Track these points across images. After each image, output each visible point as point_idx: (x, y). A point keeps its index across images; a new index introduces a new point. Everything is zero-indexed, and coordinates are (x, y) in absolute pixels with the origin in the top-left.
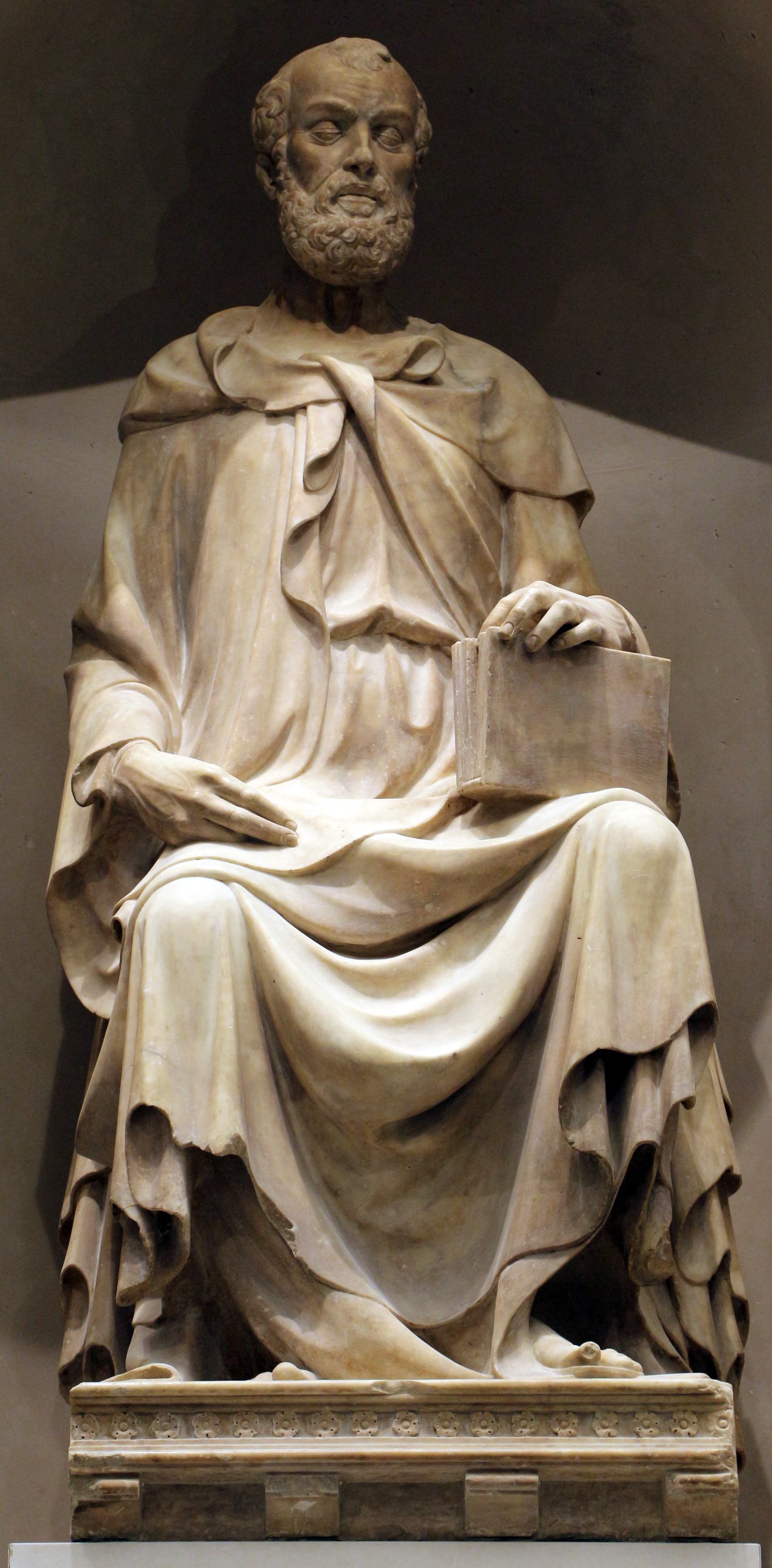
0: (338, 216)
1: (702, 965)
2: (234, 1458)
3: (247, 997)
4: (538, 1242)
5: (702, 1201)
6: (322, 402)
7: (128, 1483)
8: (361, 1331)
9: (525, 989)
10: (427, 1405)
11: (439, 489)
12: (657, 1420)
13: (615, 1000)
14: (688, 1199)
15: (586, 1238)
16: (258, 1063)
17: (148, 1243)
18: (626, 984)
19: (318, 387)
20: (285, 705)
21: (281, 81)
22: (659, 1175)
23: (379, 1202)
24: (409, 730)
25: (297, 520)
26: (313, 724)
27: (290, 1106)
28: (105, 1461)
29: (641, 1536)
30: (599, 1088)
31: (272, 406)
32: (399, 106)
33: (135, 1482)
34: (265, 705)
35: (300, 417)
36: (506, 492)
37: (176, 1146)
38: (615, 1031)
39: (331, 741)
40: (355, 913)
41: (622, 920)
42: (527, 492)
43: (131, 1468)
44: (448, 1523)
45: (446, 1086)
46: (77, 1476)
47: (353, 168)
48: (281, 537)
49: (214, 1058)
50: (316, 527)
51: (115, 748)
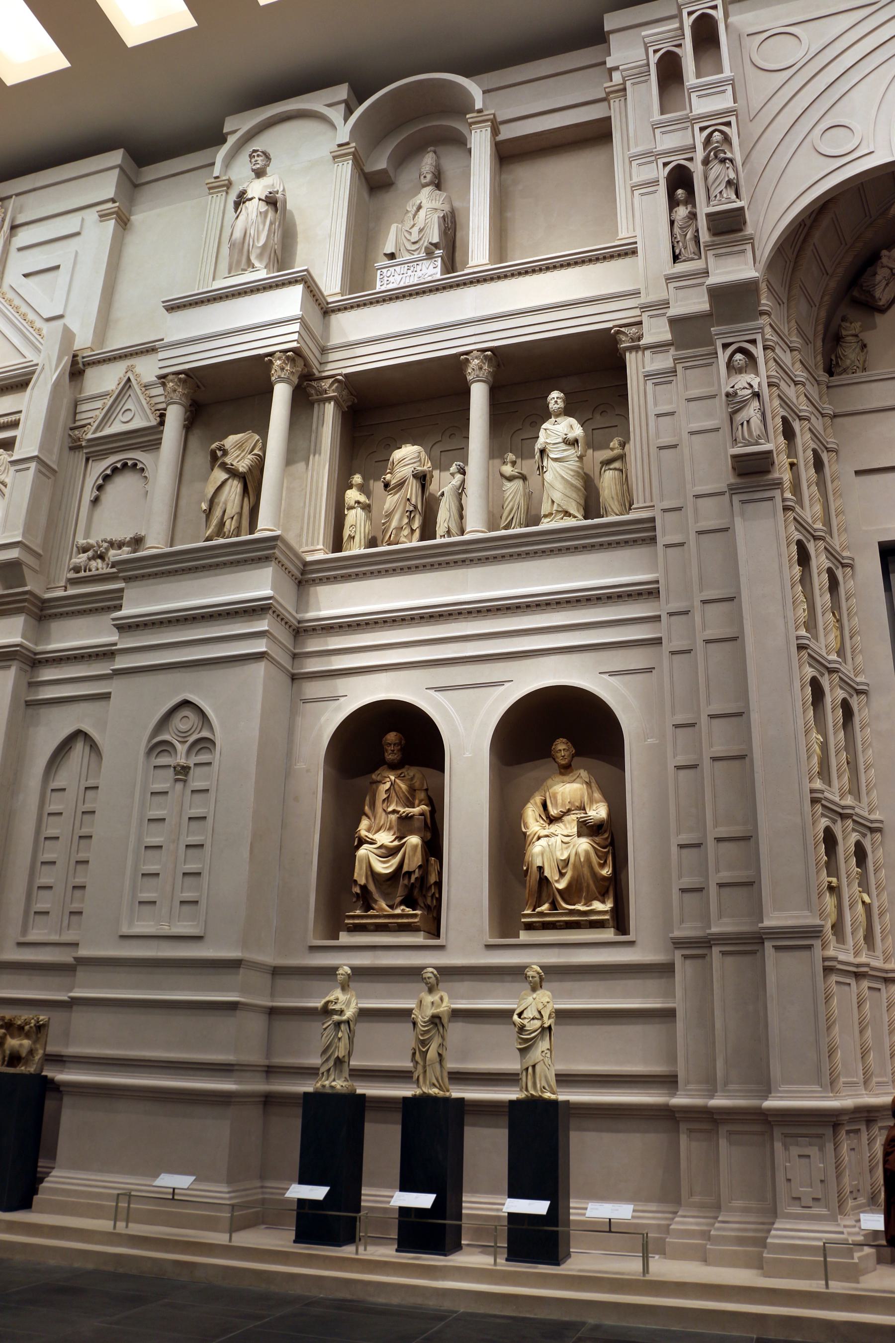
0: (390, 756)
1: (420, 859)
5: (431, 886)
18: (411, 862)
20: (382, 823)
21: (384, 739)
30: (407, 876)
32: (397, 742)
34: (379, 823)
36: (415, 790)
39: (388, 827)
40: (383, 853)
41: (411, 854)
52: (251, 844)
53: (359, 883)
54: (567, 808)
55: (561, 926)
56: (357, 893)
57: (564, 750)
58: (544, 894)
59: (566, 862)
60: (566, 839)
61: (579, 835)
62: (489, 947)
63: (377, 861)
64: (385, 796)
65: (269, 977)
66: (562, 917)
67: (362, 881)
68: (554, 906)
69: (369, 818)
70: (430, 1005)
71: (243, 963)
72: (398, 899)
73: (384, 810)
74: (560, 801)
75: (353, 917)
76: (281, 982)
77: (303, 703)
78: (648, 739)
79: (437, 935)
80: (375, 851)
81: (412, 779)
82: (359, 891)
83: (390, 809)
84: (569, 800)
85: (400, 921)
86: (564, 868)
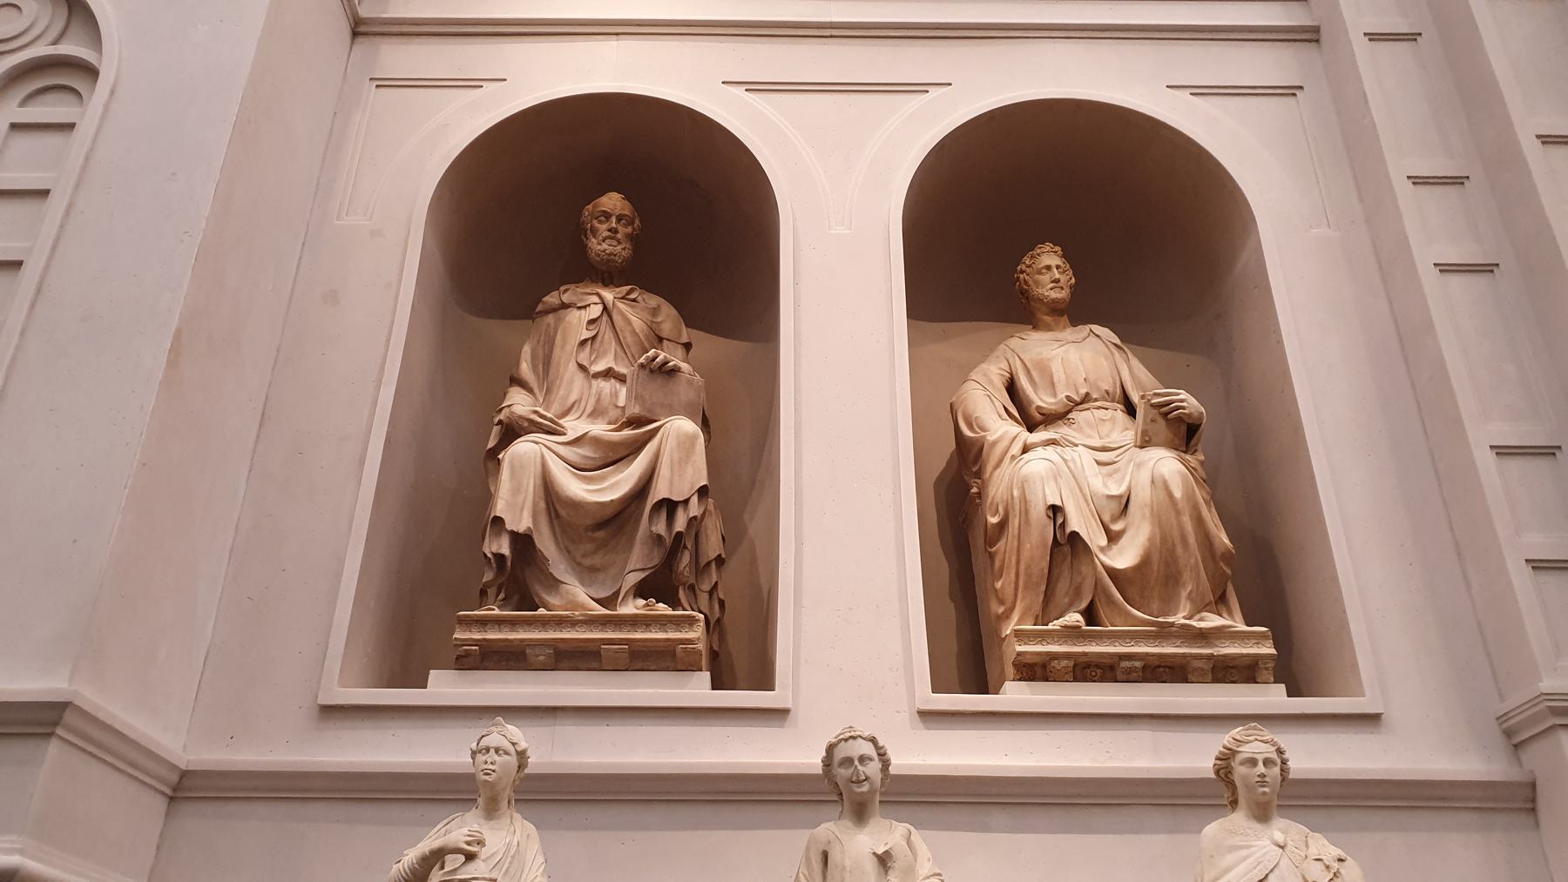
0: (605, 246)
1: (704, 472)
2: (515, 639)
3: (539, 482)
4: (638, 567)
5: (709, 564)
7: (474, 648)
8: (571, 597)
9: (640, 479)
10: (590, 621)
11: (634, 333)
12: (674, 627)
13: (671, 483)
14: (703, 562)
15: (657, 565)
16: (542, 505)
17: (494, 565)
18: (676, 478)
19: (595, 299)
20: (573, 397)
22: (685, 544)
23: (584, 556)
24: (617, 407)
25: (582, 338)
26: (583, 404)
27: (555, 522)
28: (466, 640)
29: (667, 669)
31: (579, 305)
33: (477, 648)
34: (567, 396)
37: (507, 531)
38: (671, 493)
39: (589, 410)
41: (676, 457)
43: (476, 642)
44: (595, 665)
45: (609, 512)
46: (456, 645)
48: (578, 342)
49: (524, 502)
50: (590, 342)
51: (510, 406)
52: (178, 335)
53: (509, 526)
54: (1083, 391)
55: (1130, 671)
56: (500, 558)
57: (1058, 267)
58: (1062, 587)
59: (1124, 505)
60: (1104, 456)
61: (1145, 442)
62: (929, 717)
63: (568, 475)
64: (586, 335)
65: (160, 804)
66: (1137, 643)
67: (521, 522)
68: (1090, 615)
69: (530, 390)
70: (871, 866)
71: (68, 717)
72: (633, 579)
73: (582, 367)
74: (1059, 376)
75: (483, 623)
76: (199, 823)
77: (377, 86)
78: (1311, 227)
79: (763, 679)
80: (562, 450)
81: (655, 311)
82: (505, 550)
83: (600, 367)
84: (1084, 376)
85: (638, 636)
86: (1115, 519)
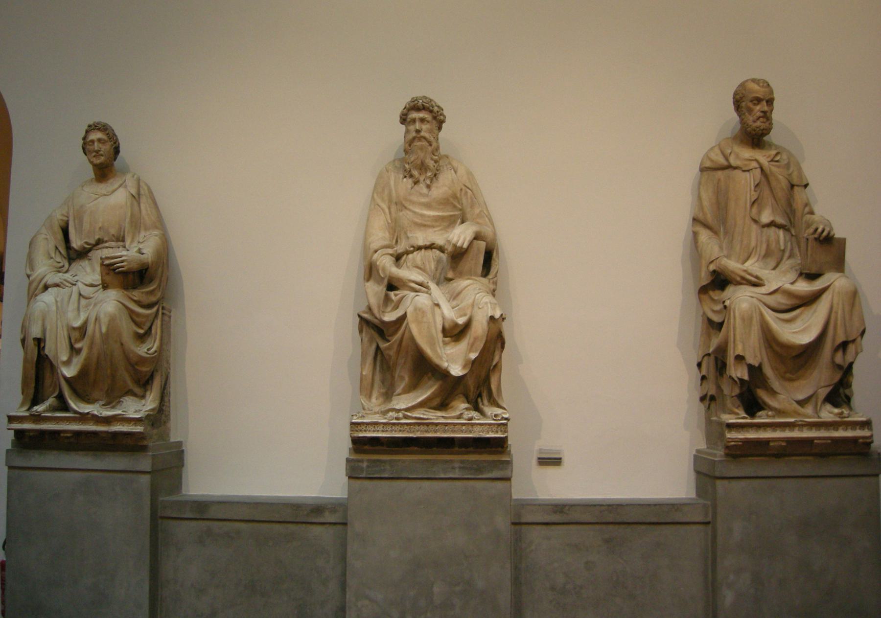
6: (756, 168)
20: (753, 244)
31: (744, 169)
35: (750, 171)
36: (792, 186)
39: (763, 253)
42: (797, 186)
47: (762, 112)
